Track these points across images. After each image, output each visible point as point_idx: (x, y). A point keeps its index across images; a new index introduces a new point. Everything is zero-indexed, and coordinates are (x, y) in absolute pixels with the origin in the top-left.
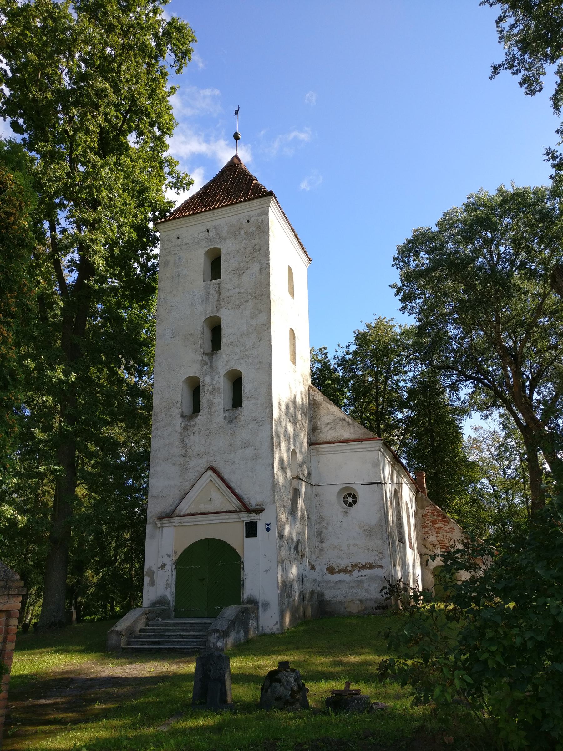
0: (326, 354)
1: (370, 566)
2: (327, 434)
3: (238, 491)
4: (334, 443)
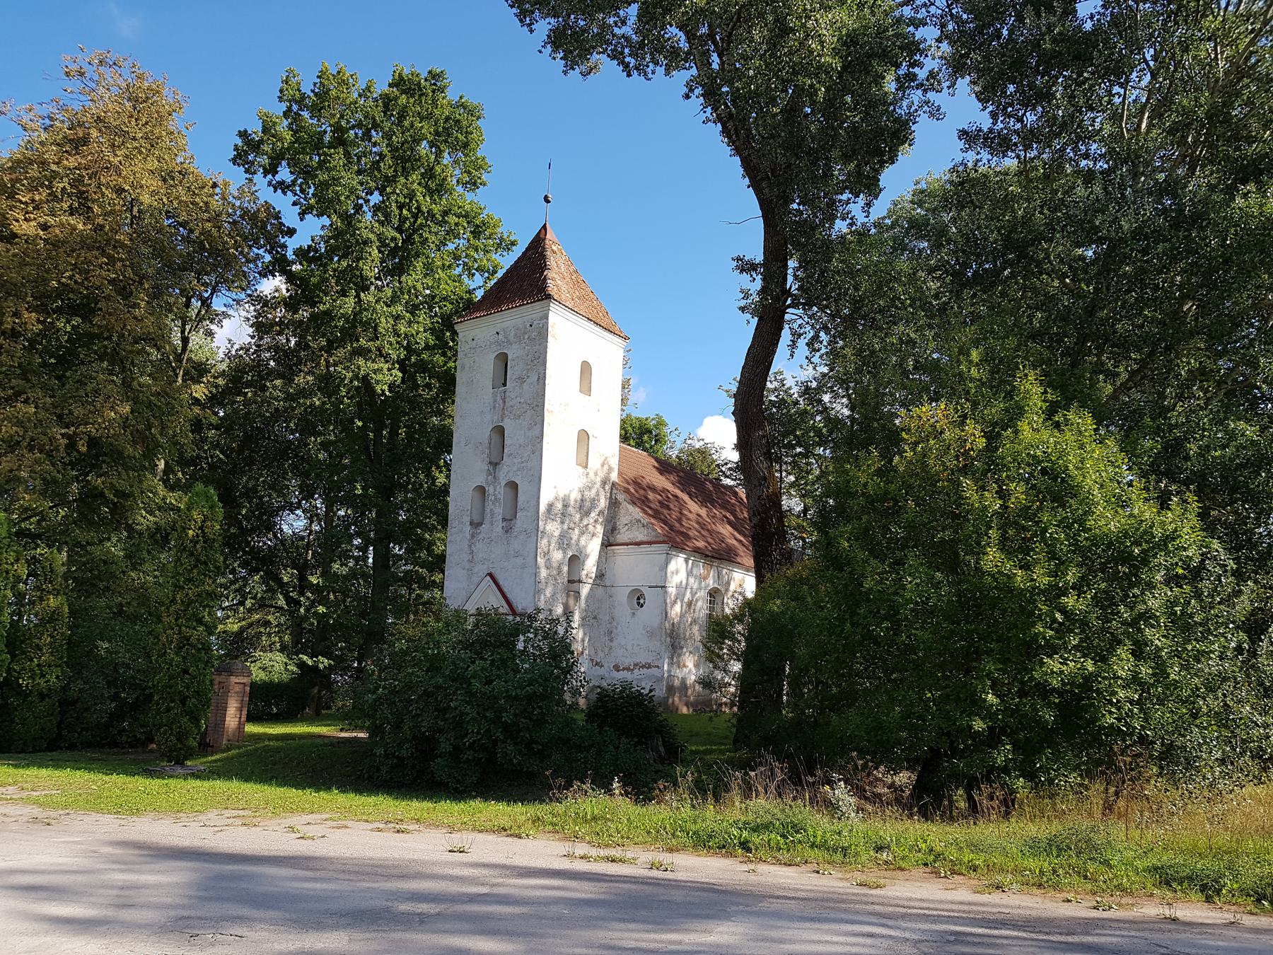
0: (782, 381)
1: (649, 666)
2: (624, 536)
3: (509, 596)
4: (627, 544)
